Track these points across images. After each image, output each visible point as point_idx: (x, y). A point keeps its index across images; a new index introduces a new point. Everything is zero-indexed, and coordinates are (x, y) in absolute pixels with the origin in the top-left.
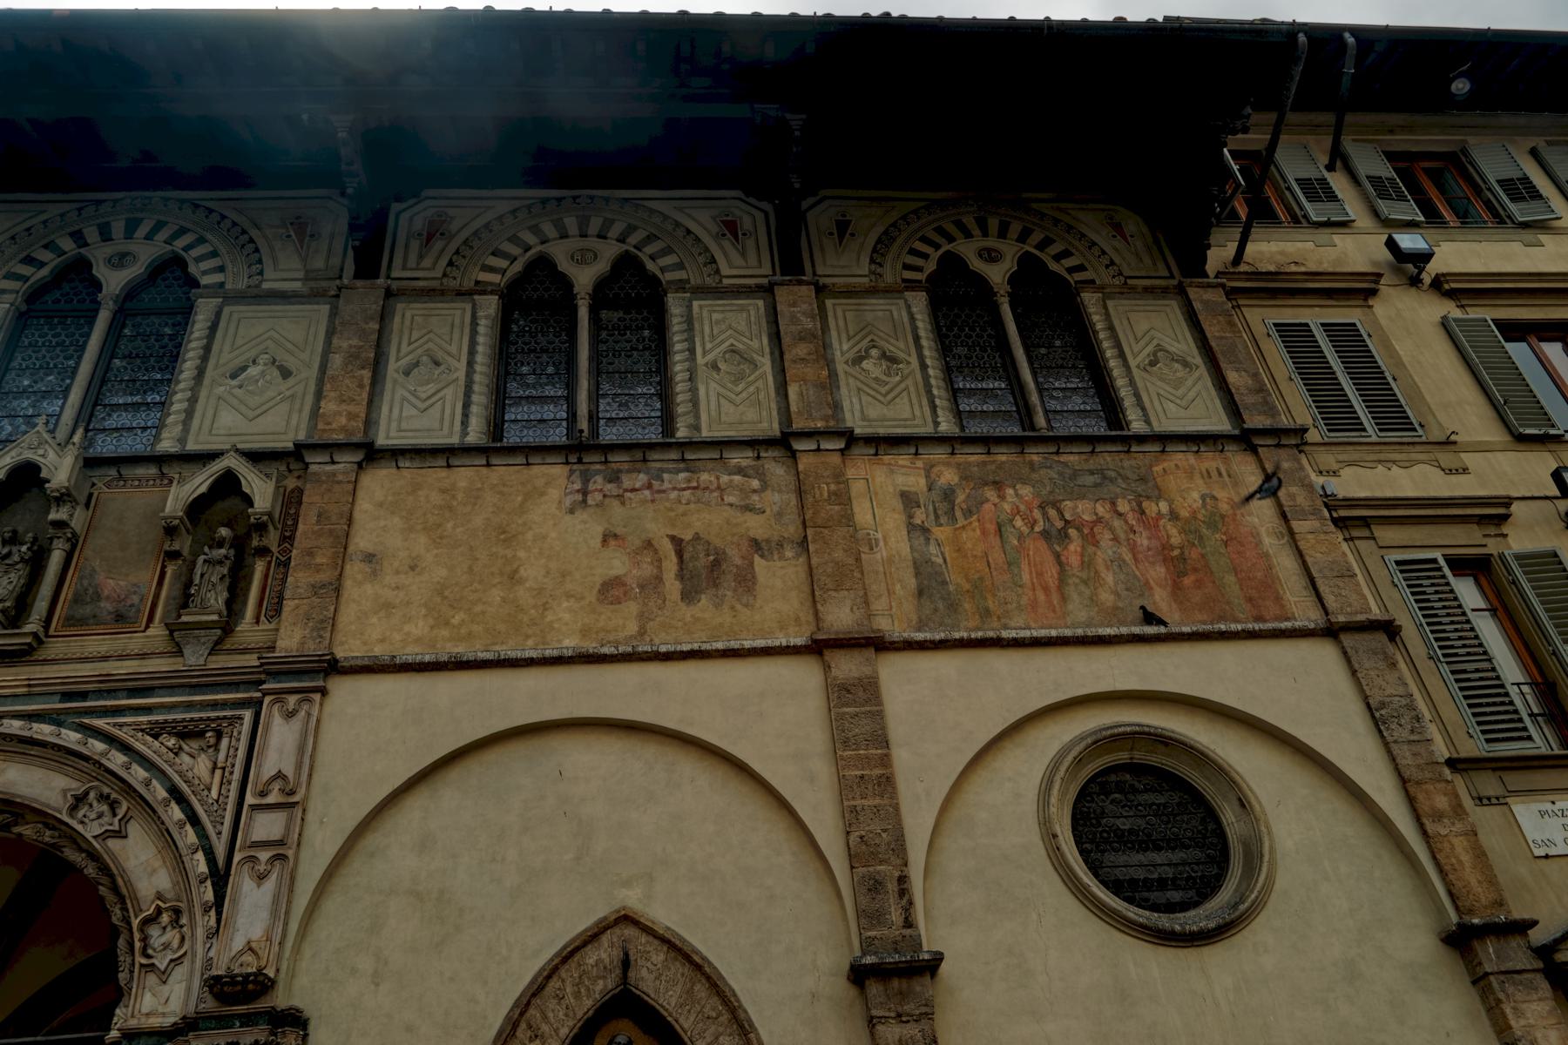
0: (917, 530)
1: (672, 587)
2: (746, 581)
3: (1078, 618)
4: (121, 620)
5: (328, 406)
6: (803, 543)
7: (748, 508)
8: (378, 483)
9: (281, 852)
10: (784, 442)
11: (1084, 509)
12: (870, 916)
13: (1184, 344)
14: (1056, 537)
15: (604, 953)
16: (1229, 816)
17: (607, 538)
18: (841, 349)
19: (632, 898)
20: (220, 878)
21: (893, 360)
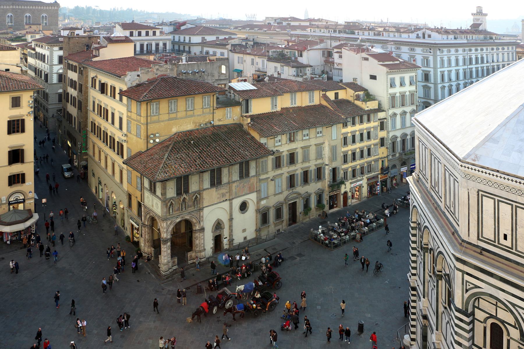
0: (236, 189)
1: (222, 197)
2: (226, 195)
3: (243, 194)
4: (191, 207)
5: (201, 187)
6: (229, 192)
7: (226, 189)
8: (205, 192)
9: (203, 220)
10: (229, 183)
11: (245, 185)
12: (230, 217)
13: (255, 166)
14: (243, 188)
15: (217, 221)
16: (247, 205)
17: (218, 194)
18: (233, 172)
19: (219, 218)
20: (200, 222)
21: (236, 172)
